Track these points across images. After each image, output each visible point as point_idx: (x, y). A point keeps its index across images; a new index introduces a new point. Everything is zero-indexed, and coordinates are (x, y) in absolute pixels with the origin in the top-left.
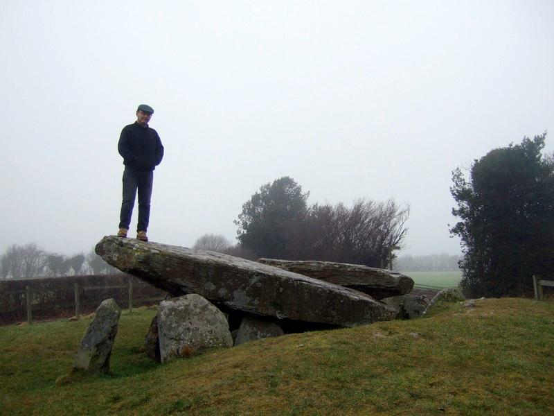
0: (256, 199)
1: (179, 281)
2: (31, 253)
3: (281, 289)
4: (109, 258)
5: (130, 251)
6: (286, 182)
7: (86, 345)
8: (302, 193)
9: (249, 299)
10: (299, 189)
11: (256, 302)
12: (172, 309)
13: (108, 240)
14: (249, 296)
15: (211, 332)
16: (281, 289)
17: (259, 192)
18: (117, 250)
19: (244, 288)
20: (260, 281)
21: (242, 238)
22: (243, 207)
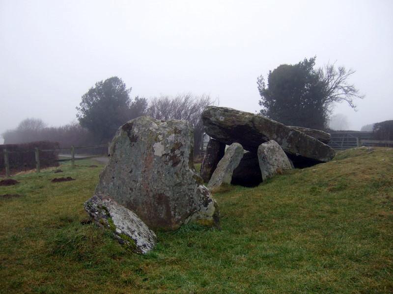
0: (92, 92)
1: (264, 133)
2: (40, 123)
3: (300, 139)
4: (217, 119)
5: (237, 115)
6: (115, 80)
7: (229, 170)
8: (127, 88)
9: (287, 144)
10: (123, 87)
11: (290, 146)
12: (269, 148)
13: (214, 108)
14: (288, 142)
15: (284, 161)
16: (300, 139)
17: (94, 87)
18: (223, 115)
19: (286, 138)
20: (292, 134)
21: (81, 120)
22: (82, 97)
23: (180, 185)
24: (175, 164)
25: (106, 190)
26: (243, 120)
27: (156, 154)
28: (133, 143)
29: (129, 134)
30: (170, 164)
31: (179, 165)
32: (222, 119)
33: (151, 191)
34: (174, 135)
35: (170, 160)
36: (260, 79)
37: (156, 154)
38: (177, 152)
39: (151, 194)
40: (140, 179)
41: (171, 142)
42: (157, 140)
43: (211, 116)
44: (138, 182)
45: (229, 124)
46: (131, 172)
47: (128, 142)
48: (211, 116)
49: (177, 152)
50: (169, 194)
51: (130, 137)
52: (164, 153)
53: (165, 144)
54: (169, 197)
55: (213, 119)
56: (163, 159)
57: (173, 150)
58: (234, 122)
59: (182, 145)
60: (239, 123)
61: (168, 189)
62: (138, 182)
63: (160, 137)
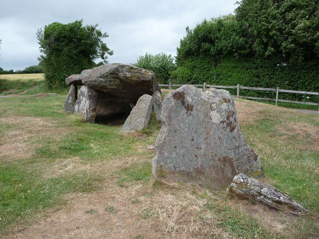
18: (129, 72)
23: (238, 147)
24: (232, 130)
25: (169, 161)
26: (147, 76)
27: (214, 121)
28: (189, 112)
29: (183, 103)
30: (228, 129)
31: (236, 130)
32: (128, 75)
33: (216, 155)
34: (225, 104)
35: (227, 126)
36: (40, 31)
37: (214, 121)
38: (232, 119)
39: (217, 159)
40: (203, 146)
41: (226, 111)
42: (212, 109)
43: (119, 72)
44: (201, 149)
45: (135, 79)
46: (193, 140)
47: (184, 111)
48: (119, 72)
49: (232, 119)
50: (232, 155)
51: (185, 107)
52: (222, 120)
53: (219, 112)
54: (232, 159)
55: (121, 75)
56: (221, 125)
57: (228, 118)
58: (139, 77)
59: (233, 112)
60: (143, 79)
61: (230, 151)
62: (201, 149)
63: (214, 105)
